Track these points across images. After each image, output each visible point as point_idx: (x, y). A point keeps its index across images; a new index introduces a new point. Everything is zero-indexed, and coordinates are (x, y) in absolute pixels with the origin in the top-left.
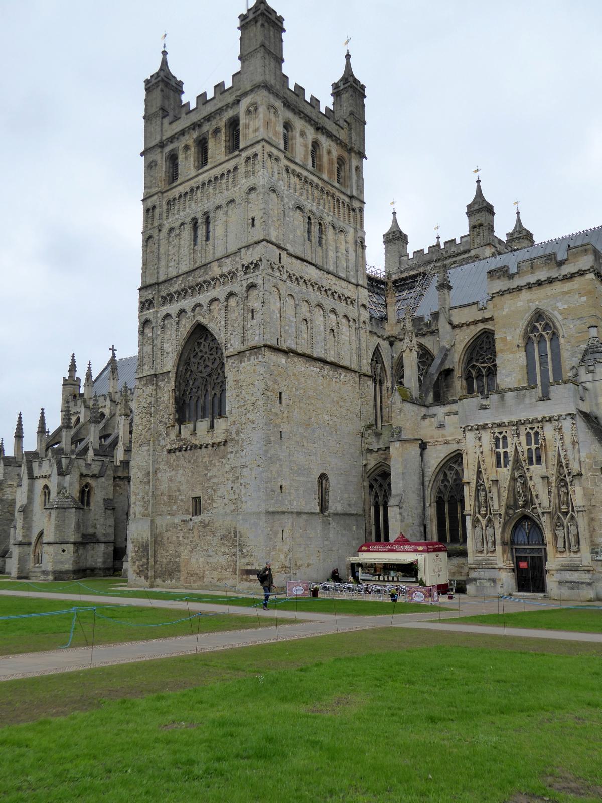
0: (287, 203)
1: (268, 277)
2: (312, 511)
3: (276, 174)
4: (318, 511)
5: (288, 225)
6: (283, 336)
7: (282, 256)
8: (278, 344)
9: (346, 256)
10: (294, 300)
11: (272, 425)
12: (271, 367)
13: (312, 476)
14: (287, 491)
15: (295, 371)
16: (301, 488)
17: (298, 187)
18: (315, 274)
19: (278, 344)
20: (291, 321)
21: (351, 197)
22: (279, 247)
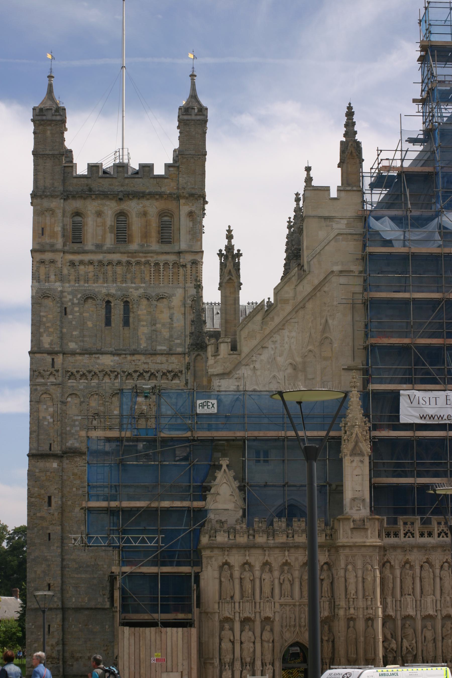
0: (70, 299)
1: (35, 387)
2: (99, 606)
3: (52, 277)
4: (108, 605)
5: (70, 322)
6: (55, 440)
7: (55, 360)
8: (50, 449)
9: (170, 324)
10: (79, 397)
11: (36, 529)
12: (36, 474)
13: (100, 572)
14: (57, 589)
15: (76, 471)
16: (82, 585)
17: (91, 275)
18: (112, 361)
19: (50, 449)
20: (75, 421)
21: (179, 253)
22: (49, 353)
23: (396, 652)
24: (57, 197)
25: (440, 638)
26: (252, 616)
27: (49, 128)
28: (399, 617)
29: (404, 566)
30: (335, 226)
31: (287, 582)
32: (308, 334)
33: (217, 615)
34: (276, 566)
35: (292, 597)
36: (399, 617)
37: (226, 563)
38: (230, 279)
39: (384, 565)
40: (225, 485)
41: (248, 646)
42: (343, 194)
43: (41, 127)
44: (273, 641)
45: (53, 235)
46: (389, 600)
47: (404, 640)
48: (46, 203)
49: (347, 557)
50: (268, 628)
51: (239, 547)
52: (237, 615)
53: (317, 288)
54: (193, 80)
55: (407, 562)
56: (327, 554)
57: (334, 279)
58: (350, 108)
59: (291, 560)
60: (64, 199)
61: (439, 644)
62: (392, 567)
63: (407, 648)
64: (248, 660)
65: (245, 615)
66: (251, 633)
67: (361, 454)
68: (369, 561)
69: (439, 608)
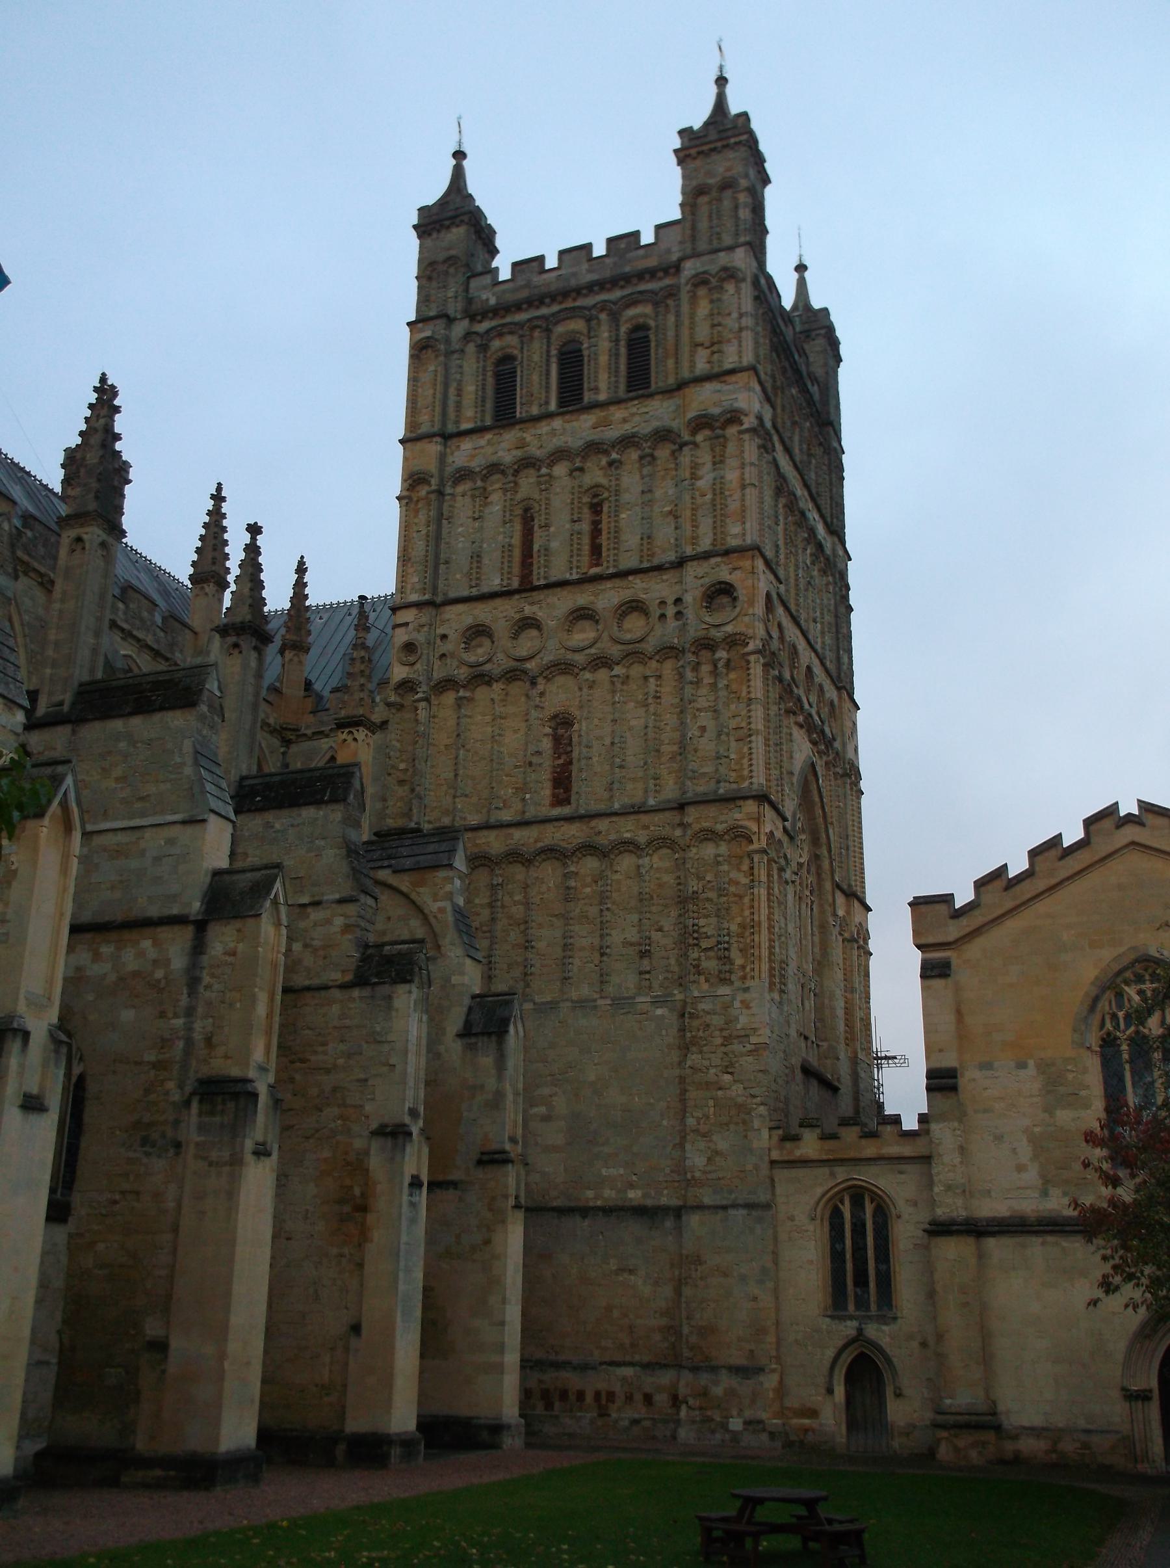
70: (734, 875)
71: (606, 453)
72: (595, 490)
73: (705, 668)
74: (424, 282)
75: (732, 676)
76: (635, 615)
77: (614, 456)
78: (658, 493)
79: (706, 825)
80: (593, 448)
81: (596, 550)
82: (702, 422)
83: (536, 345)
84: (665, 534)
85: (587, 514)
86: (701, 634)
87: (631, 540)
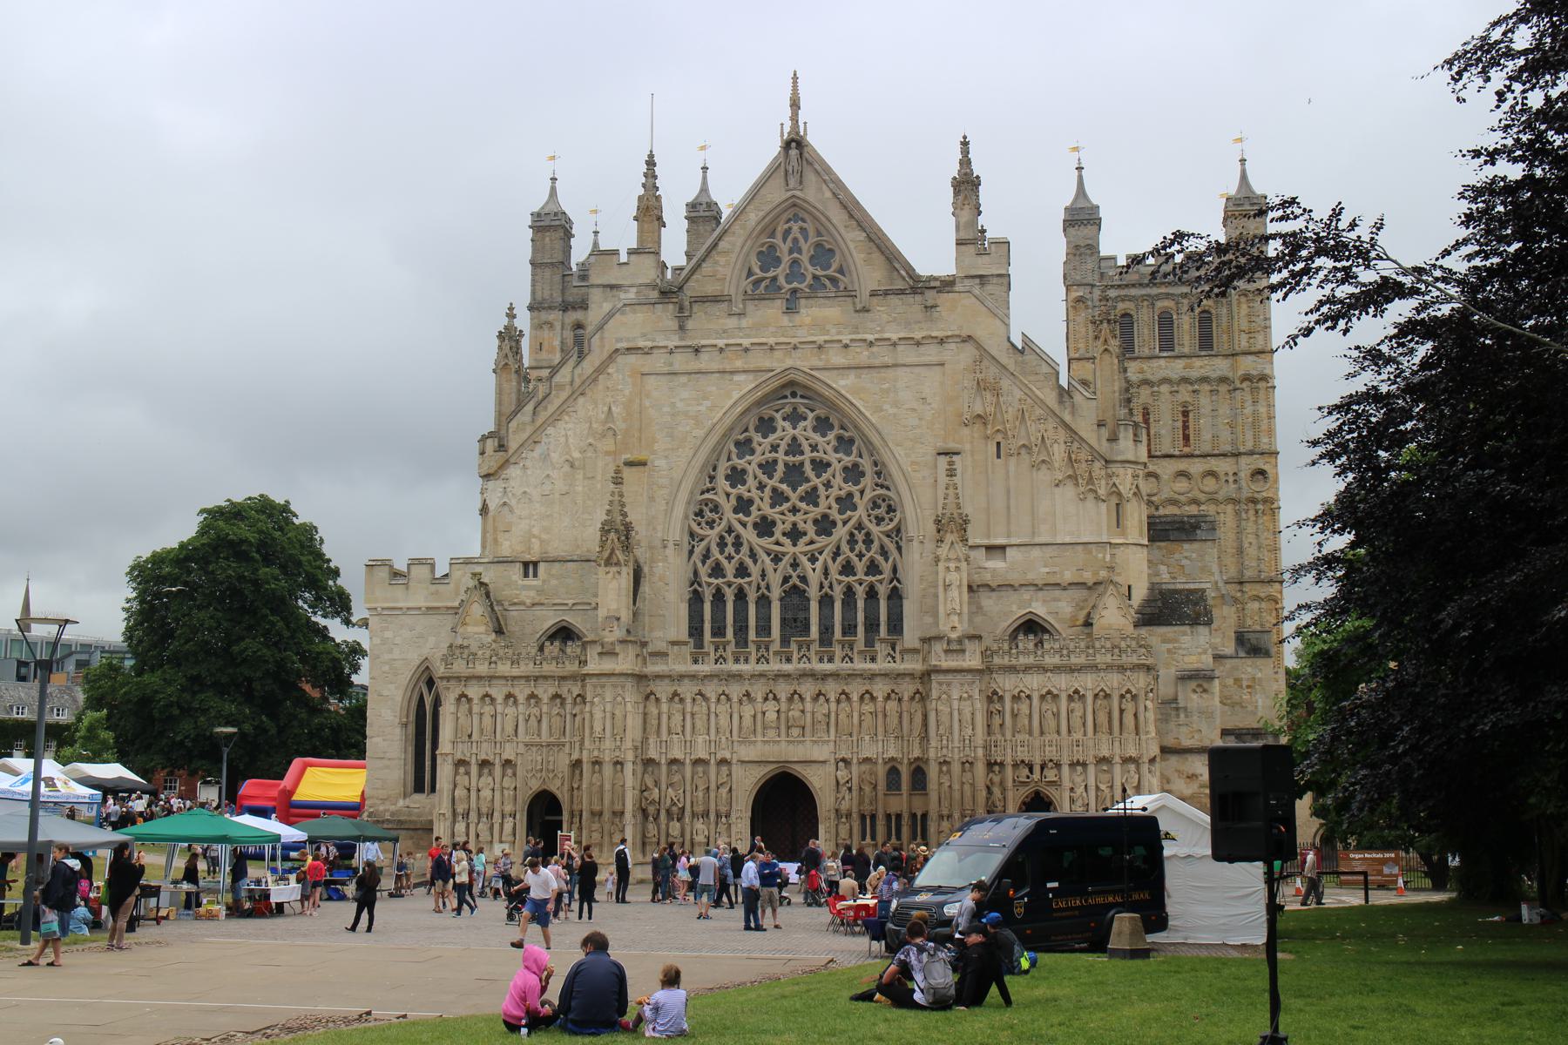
23: (659, 803)
24: (555, 308)
25: (713, 786)
26: (491, 758)
27: (548, 234)
28: (663, 761)
29: (672, 699)
30: (623, 296)
31: (532, 718)
32: (588, 425)
33: (450, 757)
34: (521, 698)
35: (539, 735)
36: (663, 761)
37: (463, 695)
38: (506, 364)
39: (647, 698)
40: (476, 605)
41: (486, 793)
42: (633, 257)
43: (539, 234)
44: (515, 788)
45: (552, 351)
46: (651, 741)
47: (670, 790)
48: (544, 316)
49: (595, 687)
50: (509, 772)
51: (480, 678)
52: (474, 757)
53: (600, 370)
54: (705, 173)
55: (675, 694)
56: (579, 683)
57: (620, 359)
58: (651, 156)
59: (539, 692)
60: (564, 311)
61: (712, 795)
62: (657, 700)
63: (672, 800)
64: (484, 810)
65: (483, 756)
66: (490, 779)
67: (618, 564)
68: (621, 692)
69: (713, 750)
70: (1268, 618)
71: (1191, 384)
72: (1185, 404)
73: (1252, 512)
74: (1071, 256)
75: (1265, 518)
76: (1209, 477)
77: (1196, 387)
78: (1221, 412)
79: (1255, 593)
80: (1185, 380)
81: (1186, 438)
82: (1247, 378)
83: (1145, 310)
84: (1225, 435)
85: (1181, 418)
86: (1250, 495)
87: (1207, 436)
